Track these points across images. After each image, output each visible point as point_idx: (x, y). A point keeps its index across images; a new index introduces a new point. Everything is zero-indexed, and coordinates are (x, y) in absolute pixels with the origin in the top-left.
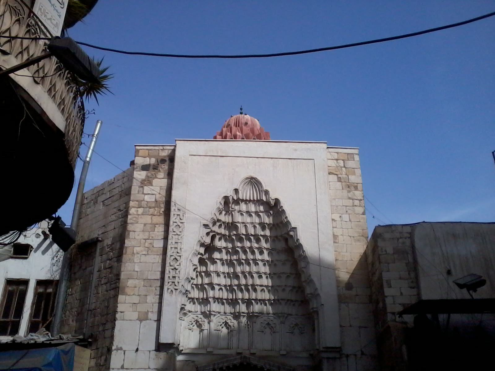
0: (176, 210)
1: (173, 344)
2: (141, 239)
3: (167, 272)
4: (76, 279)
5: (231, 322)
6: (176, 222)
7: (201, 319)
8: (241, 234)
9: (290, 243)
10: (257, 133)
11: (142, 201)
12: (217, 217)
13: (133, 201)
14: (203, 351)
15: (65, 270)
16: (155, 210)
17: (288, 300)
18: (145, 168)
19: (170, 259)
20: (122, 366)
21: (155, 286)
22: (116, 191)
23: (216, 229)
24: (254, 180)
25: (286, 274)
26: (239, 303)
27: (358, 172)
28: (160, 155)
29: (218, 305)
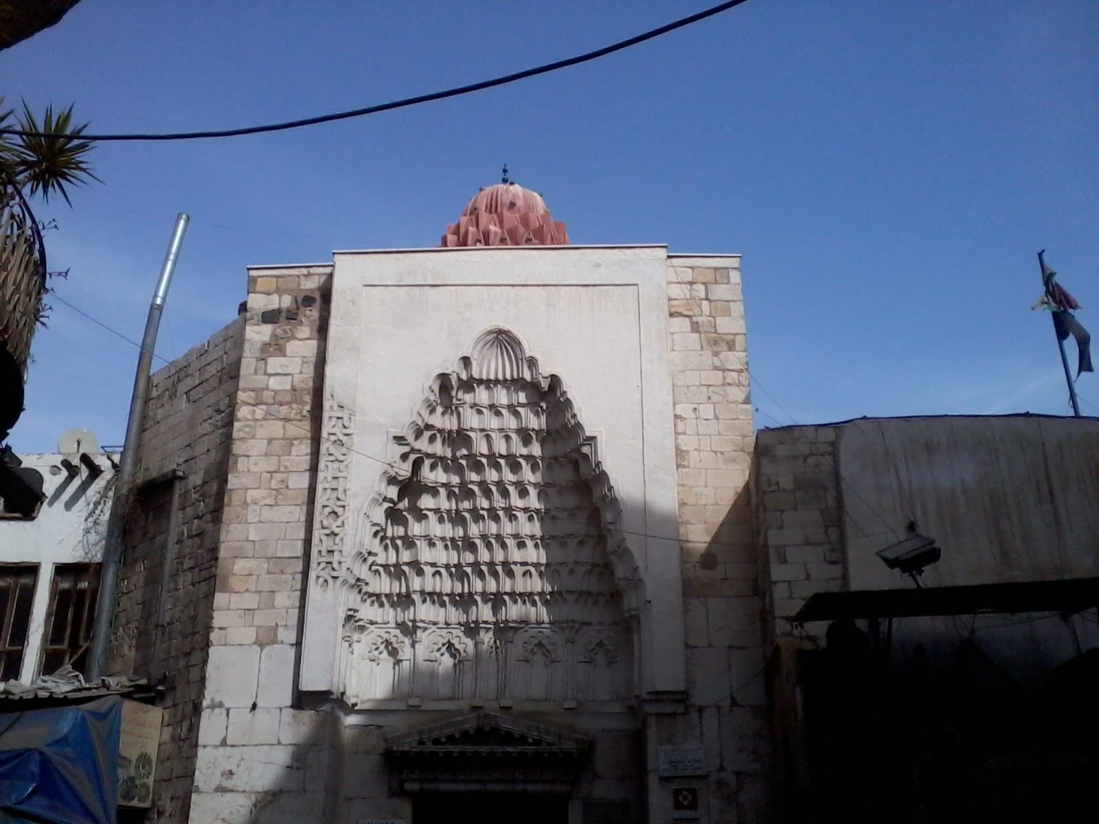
0: (335, 407)
1: (329, 693)
2: (261, 473)
3: (315, 541)
4: (136, 561)
5: (460, 643)
6: (334, 434)
7: (395, 638)
8: (478, 454)
9: (583, 469)
10: (535, 224)
11: (263, 389)
12: (423, 420)
13: (244, 390)
14: (403, 706)
15: (113, 541)
16: (292, 408)
17: (581, 593)
18: (270, 317)
19: (321, 513)
20: (223, 739)
21: (290, 571)
22: (213, 369)
23: (423, 444)
24: (504, 335)
25: (576, 537)
26: (476, 603)
27: (738, 308)
28: (302, 287)
29: (432, 607)
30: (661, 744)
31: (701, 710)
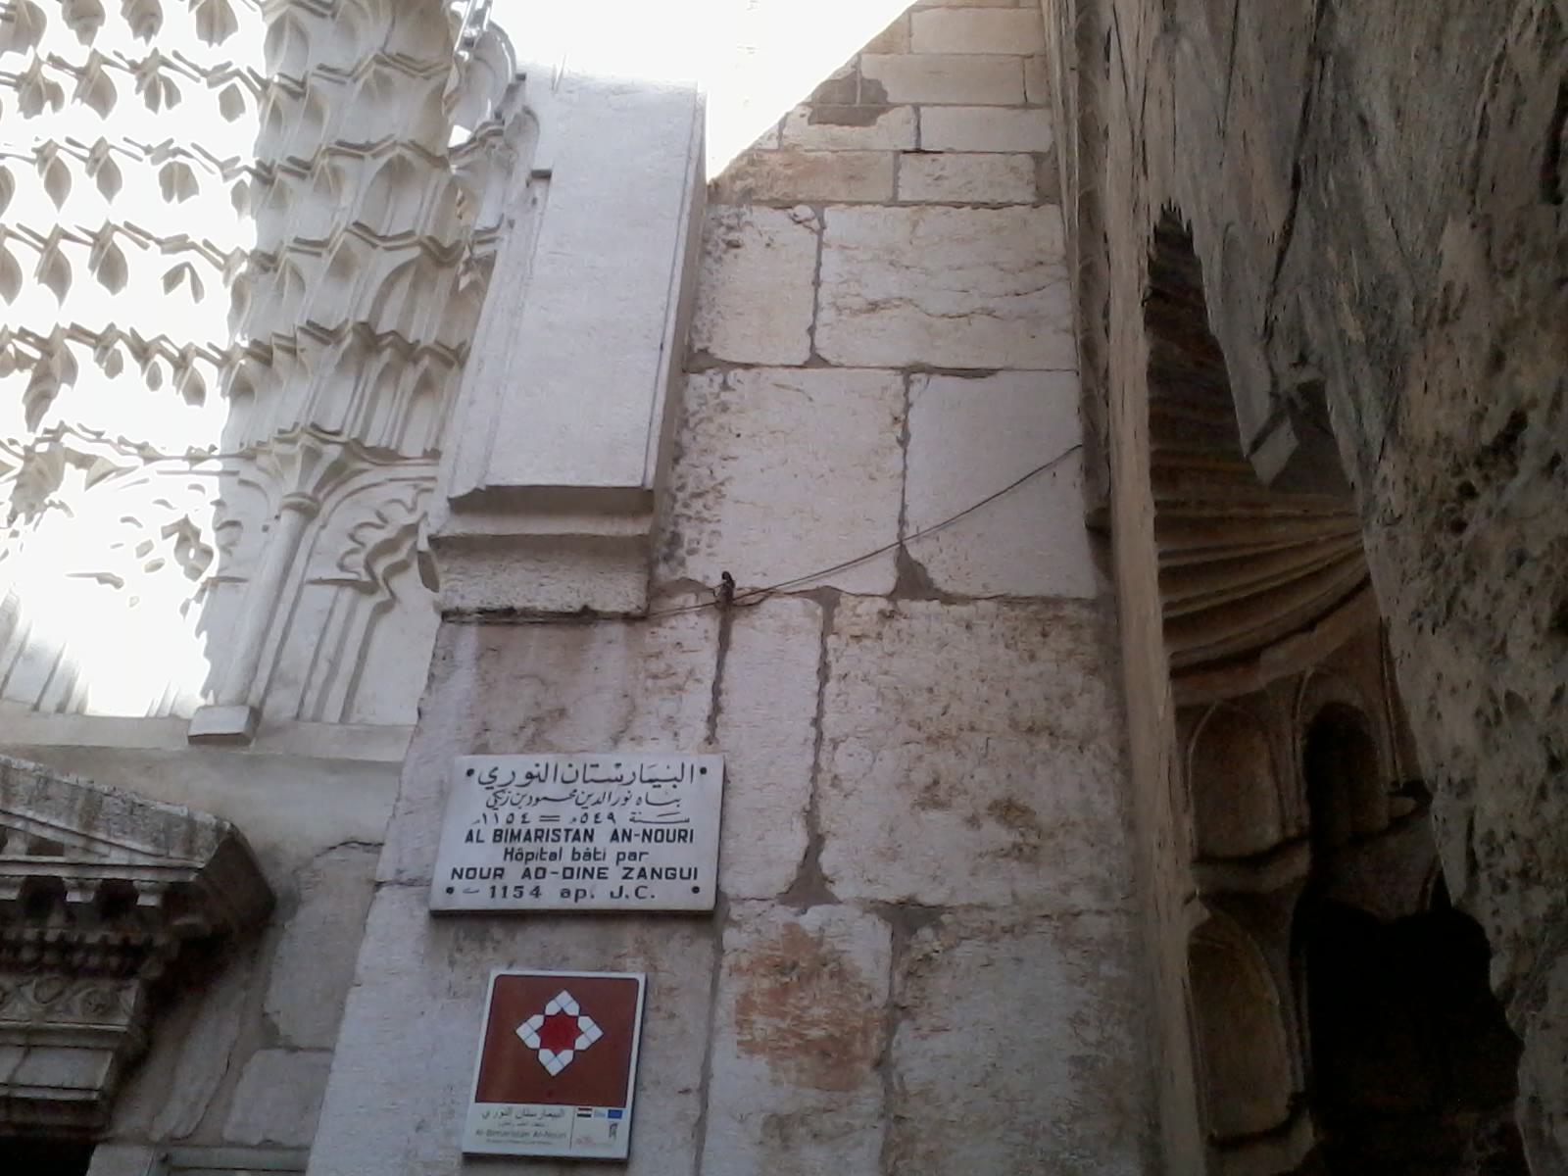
30: (483, 749)
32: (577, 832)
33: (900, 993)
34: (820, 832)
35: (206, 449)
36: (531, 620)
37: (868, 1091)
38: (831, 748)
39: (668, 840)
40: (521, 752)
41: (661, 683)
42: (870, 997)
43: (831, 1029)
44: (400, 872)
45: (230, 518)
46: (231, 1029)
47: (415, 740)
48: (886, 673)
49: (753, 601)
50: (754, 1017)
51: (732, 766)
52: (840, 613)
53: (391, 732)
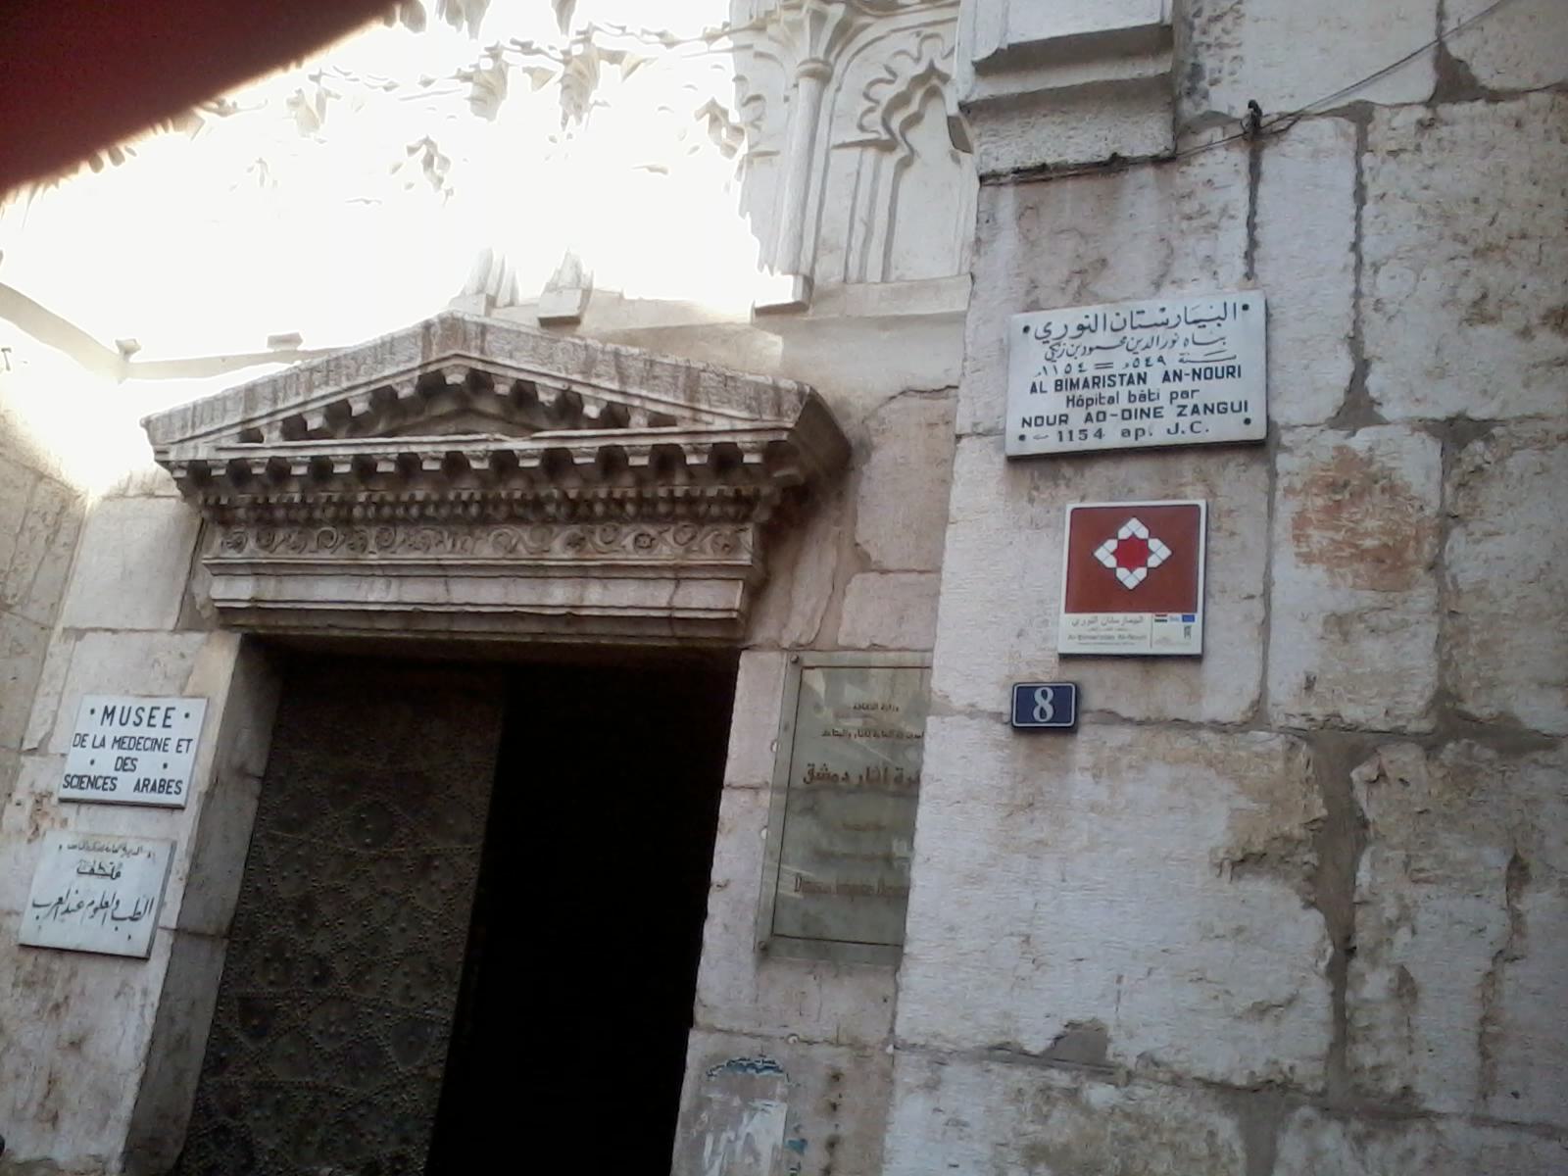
30: (1033, 306)
31: (1257, 132)
32: (1131, 376)
33: (1451, 504)
34: (1365, 356)
35: (720, 27)
36: (1062, 174)
37: (1422, 591)
38: (1371, 272)
39: (1217, 377)
40: (1066, 307)
41: (1195, 223)
42: (1421, 508)
43: (1385, 539)
44: (975, 425)
45: (751, 93)
46: (831, 558)
47: (973, 302)
48: (1426, 188)
49: (1282, 128)
50: (1311, 531)
51: (1274, 301)
52: (1375, 128)
53: (931, 286)
